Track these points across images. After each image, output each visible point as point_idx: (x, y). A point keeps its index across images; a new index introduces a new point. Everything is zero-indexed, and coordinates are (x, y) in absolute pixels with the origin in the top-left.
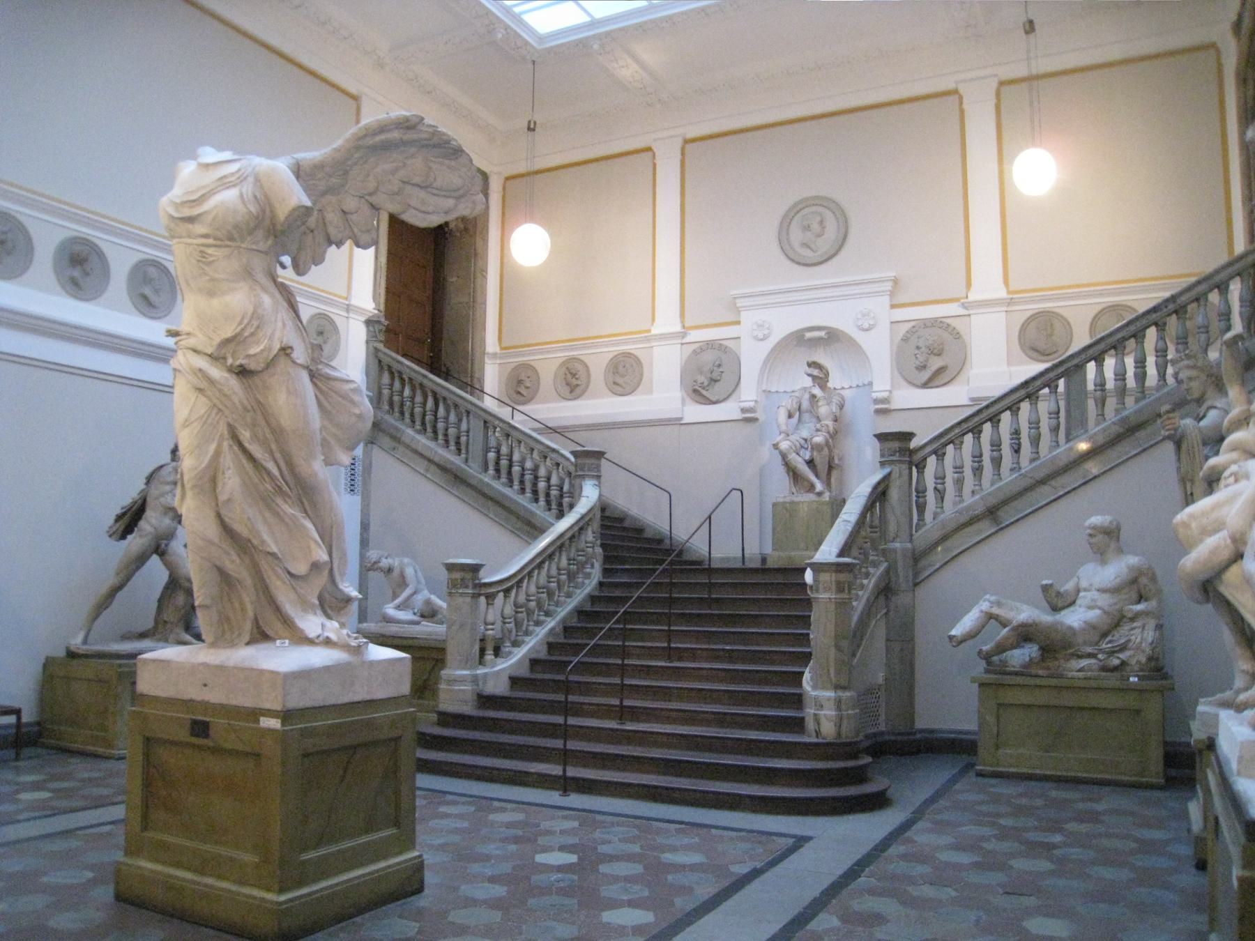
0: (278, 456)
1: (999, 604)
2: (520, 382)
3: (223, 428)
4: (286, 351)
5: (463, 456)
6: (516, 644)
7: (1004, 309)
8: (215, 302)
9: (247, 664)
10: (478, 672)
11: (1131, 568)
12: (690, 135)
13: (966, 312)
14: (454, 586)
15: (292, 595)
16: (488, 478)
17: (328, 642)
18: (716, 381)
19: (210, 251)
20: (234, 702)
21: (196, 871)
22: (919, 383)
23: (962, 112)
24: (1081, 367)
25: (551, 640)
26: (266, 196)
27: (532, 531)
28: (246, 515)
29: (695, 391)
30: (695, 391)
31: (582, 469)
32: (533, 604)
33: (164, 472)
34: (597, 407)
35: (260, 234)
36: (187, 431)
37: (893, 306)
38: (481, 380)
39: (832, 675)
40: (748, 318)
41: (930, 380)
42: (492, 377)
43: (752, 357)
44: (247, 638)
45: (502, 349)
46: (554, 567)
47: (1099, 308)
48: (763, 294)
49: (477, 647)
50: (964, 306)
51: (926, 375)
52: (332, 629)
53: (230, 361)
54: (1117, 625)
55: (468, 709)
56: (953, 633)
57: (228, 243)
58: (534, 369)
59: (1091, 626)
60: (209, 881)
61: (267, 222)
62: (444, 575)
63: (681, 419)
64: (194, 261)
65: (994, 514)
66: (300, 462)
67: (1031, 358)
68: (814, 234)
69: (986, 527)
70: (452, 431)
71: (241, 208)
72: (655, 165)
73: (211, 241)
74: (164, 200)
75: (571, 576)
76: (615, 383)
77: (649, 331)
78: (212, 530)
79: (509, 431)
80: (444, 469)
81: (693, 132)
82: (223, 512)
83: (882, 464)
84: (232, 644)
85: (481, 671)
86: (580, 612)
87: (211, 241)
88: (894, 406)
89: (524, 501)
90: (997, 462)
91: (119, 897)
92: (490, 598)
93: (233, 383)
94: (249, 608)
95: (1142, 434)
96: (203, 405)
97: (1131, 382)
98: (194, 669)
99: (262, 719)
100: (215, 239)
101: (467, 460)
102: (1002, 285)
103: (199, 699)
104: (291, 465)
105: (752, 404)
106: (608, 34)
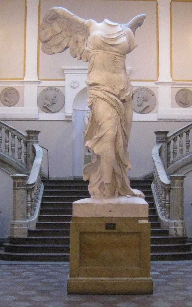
7: (171, 86)
8: (115, 75)
10: (27, 221)
18: (54, 103)
19: (117, 57)
22: (138, 111)
23: (157, 9)
27: (3, 164)
29: (45, 107)
30: (45, 107)
36: (110, 121)
39: (180, 215)
40: (69, 79)
41: (144, 110)
43: (70, 95)
48: (72, 69)
50: (156, 83)
51: (141, 109)
55: (26, 236)
57: (123, 56)
63: (38, 118)
64: (110, 60)
67: (180, 106)
73: (118, 54)
76: (6, 101)
77: (23, 79)
78: (113, 156)
83: (158, 143)
85: (28, 221)
87: (118, 54)
98: (104, 206)
99: (139, 221)
100: (120, 54)
102: (170, 77)
103: (108, 216)
105: (71, 114)
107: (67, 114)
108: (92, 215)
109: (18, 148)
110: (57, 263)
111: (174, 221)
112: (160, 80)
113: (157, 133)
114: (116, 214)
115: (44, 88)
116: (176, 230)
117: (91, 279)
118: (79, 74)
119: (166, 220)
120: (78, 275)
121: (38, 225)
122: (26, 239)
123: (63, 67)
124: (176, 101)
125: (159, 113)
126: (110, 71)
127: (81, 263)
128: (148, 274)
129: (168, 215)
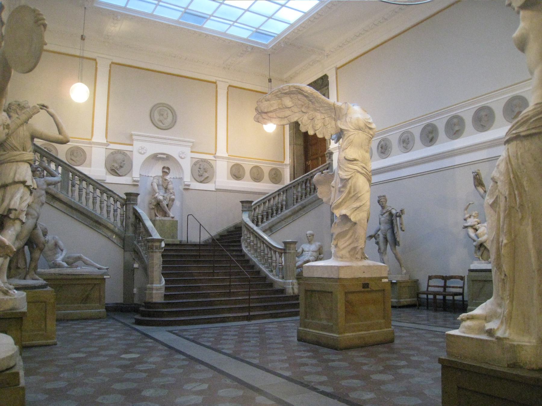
11: (319, 245)
13: (215, 159)
18: (121, 167)
21: (366, 330)
27: (98, 226)
29: (112, 170)
30: (112, 170)
37: (192, 152)
40: (137, 145)
43: (138, 161)
47: (252, 166)
50: (215, 157)
51: (202, 179)
55: (162, 301)
60: (372, 331)
63: (105, 180)
68: (163, 118)
88: (190, 188)
95: (305, 209)
103: (363, 277)
107: (134, 179)
108: (352, 276)
109: (114, 210)
111: (291, 281)
112: (217, 154)
113: (242, 202)
114: (367, 275)
115: (113, 151)
116: (293, 289)
117: (354, 334)
118: (150, 142)
119: (280, 280)
123: (133, 133)
125: (217, 184)
128: (388, 325)
129: (281, 276)
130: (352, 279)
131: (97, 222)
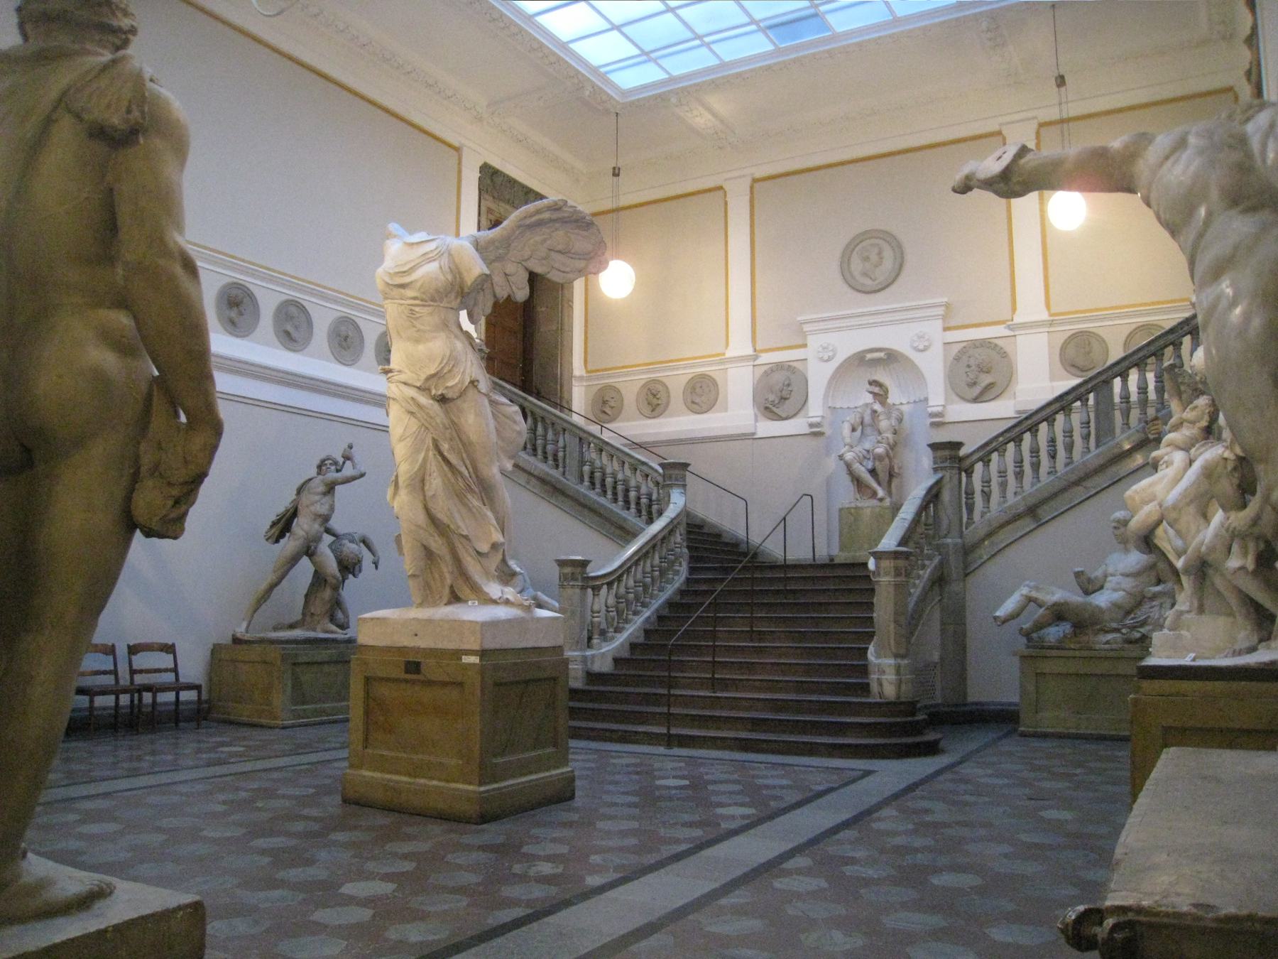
0: (468, 462)
1: (1037, 589)
2: (605, 402)
3: (429, 442)
4: (473, 383)
5: (561, 469)
6: (618, 630)
8: (421, 347)
9: (451, 617)
12: (757, 175)
14: (566, 579)
15: (479, 567)
16: (584, 489)
17: (507, 602)
19: (417, 309)
20: (440, 646)
21: (410, 775)
24: (1108, 383)
25: (648, 627)
26: (457, 268)
28: (444, 507)
30: (766, 408)
31: (670, 477)
32: (631, 596)
33: (312, 484)
34: (678, 423)
35: (453, 295)
36: (402, 444)
37: (946, 329)
38: (570, 401)
40: (815, 342)
41: (982, 393)
42: (579, 398)
43: (818, 377)
44: (445, 600)
45: (588, 372)
46: (648, 564)
49: (585, 633)
50: (1009, 327)
51: (977, 390)
52: (510, 593)
53: (433, 392)
54: (1139, 604)
56: (997, 614)
58: (618, 391)
59: (1116, 605)
60: (422, 781)
61: (457, 287)
62: (556, 570)
63: (754, 434)
65: (1034, 512)
66: (480, 466)
68: (873, 264)
69: (1027, 524)
70: (549, 447)
71: (442, 277)
72: (726, 203)
74: (380, 270)
75: (663, 572)
78: (421, 518)
79: (602, 446)
80: (543, 481)
81: (759, 173)
82: (430, 505)
84: (435, 604)
85: (589, 653)
86: (670, 604)
88: (947, 419)
89: (617, 508)
90: (1036, 466)
91: (346, 801)
92: (596, 589)
93: (436, 406)
94: (447, 575)
96: (414, 425)
97: (1152, 395)
101: (564, 473)
104: (475, 469)
105: (818, 420)
106: (684, 89)
110: (593, 745)
114: (423, 643)
115: (766, 368)
120: (360, 767)
121: (617, 661)
122: (583, 691)
124: (1062, 364)
126: (409, 339)
127: (366, 742)
130: (388, 650)
131: (621, 528)
